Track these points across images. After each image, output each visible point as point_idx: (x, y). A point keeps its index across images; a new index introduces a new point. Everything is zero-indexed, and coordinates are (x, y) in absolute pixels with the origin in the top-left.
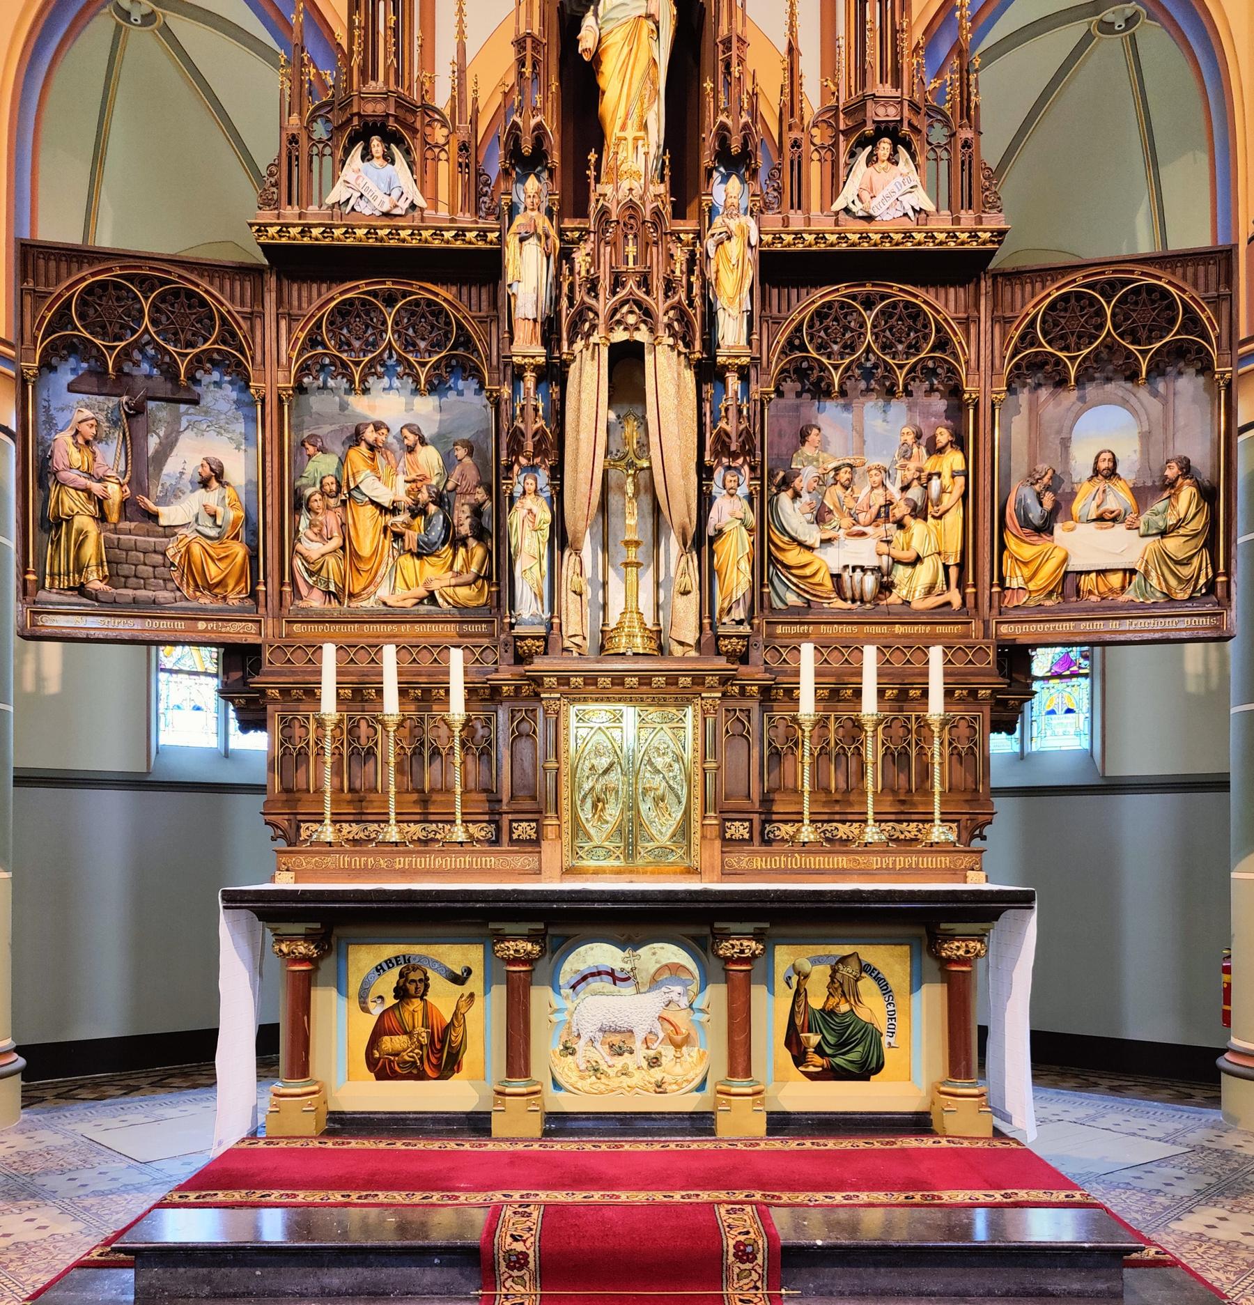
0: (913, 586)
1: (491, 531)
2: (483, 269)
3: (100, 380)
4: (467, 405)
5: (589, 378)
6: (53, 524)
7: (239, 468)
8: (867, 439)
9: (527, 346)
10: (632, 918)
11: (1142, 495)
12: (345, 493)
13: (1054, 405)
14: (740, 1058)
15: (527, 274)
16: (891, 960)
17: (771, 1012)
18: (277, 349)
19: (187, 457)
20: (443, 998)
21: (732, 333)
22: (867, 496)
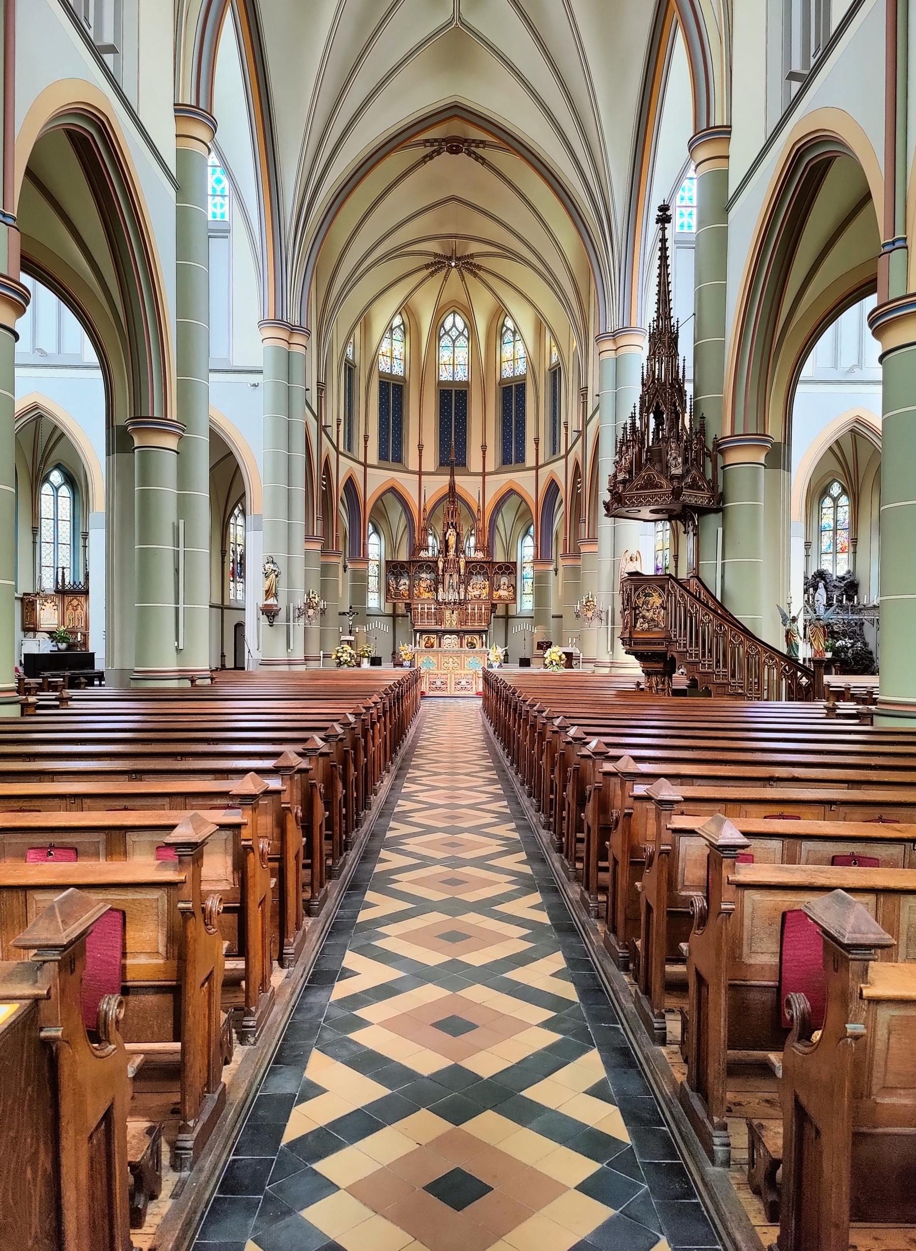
0: (483, 597)
1: (436, 590)
2: (436, 562)
3: (393, 574)
4: (433, 575)
5: (447, 577)
6: (389, 590)
7: (407, 583)
8: (478, 580)
9: (440, 573)
10: (451, 632)
11: (508, 587)
12: (419, 585)
13: (499, 576)
14: (461, 646)
15: (441, 565)
16: (477, 637)
17: (465, 642)
18: (413, 569)
19: (402, 582)
20: (432, 640)
21: (462, 571)
22: (478, 586)
